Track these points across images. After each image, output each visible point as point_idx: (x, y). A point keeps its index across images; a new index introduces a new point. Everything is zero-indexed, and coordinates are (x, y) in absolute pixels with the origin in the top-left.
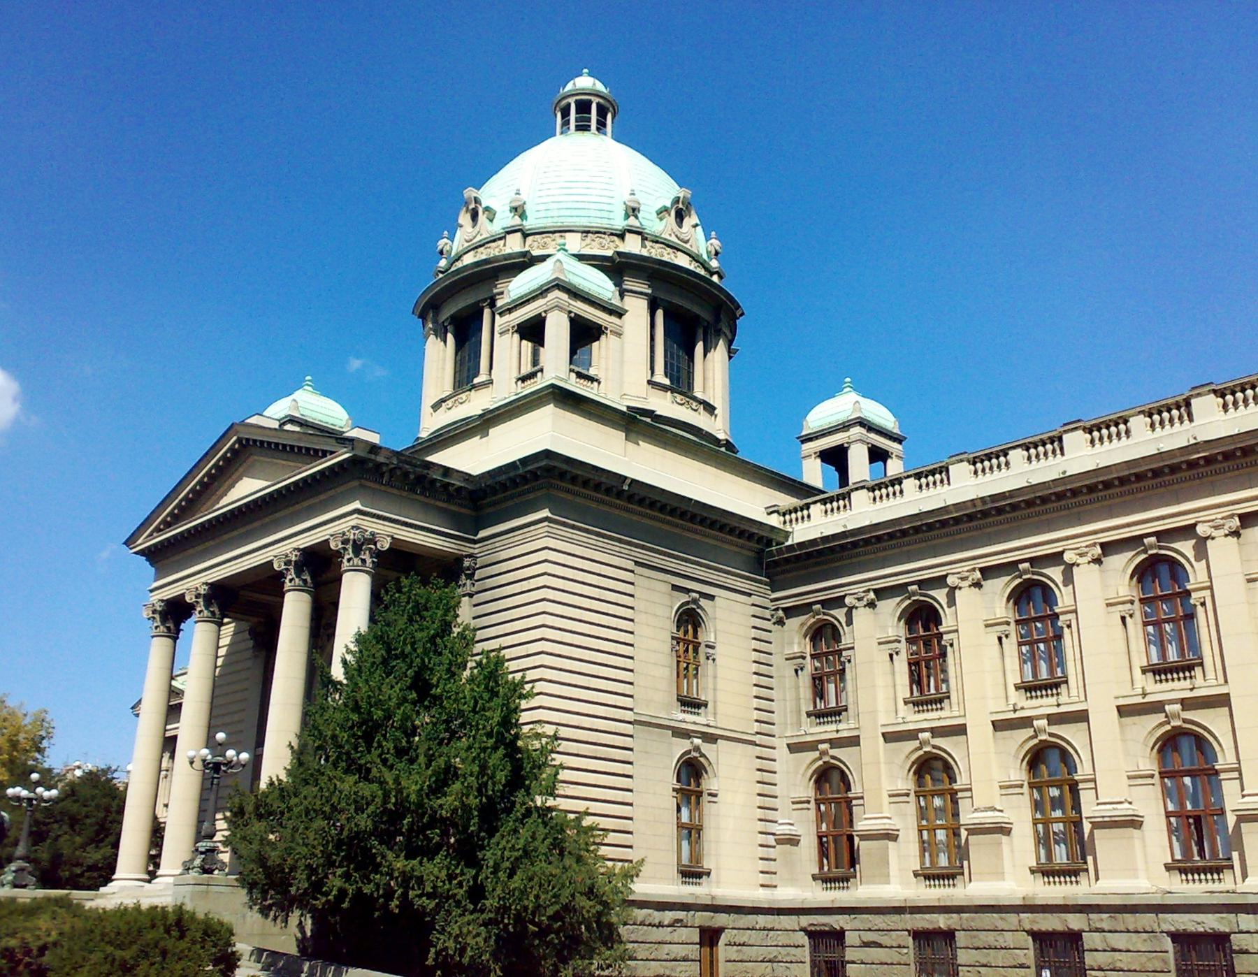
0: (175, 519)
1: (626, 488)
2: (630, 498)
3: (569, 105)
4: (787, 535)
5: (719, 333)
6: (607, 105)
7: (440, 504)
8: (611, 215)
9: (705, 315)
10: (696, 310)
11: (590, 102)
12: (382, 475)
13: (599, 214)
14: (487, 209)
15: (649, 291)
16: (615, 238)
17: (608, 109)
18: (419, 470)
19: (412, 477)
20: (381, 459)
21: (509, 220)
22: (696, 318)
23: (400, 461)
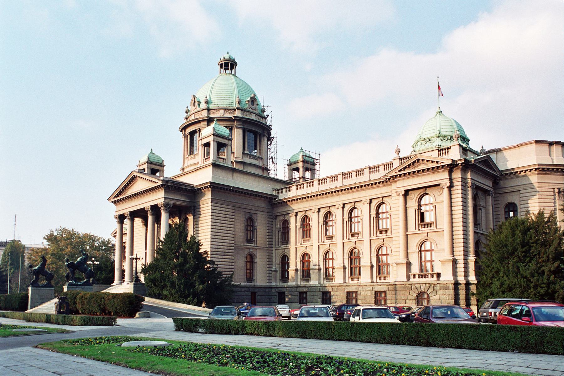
0: (118, 195)
1: (232, 189)
2: (233, 191)
3: (222, 64)
4: (277, 196)
5: (264, 136)
6: (234, 63)
7: (186, 194)
8: (233, 104)
9: (259, 131)
10: (257, 130)
11: (228, 63)
12: (170, 188)
13: (229, 103)
14: (198, 101)
15: (243, 127)
16: (233, 111)
17: (234, 64)
18: (179, 186)
19: (177, 188)
20: (169, 184)
21: (203, 106)
22: (257, 132)
23: (174, 184)
